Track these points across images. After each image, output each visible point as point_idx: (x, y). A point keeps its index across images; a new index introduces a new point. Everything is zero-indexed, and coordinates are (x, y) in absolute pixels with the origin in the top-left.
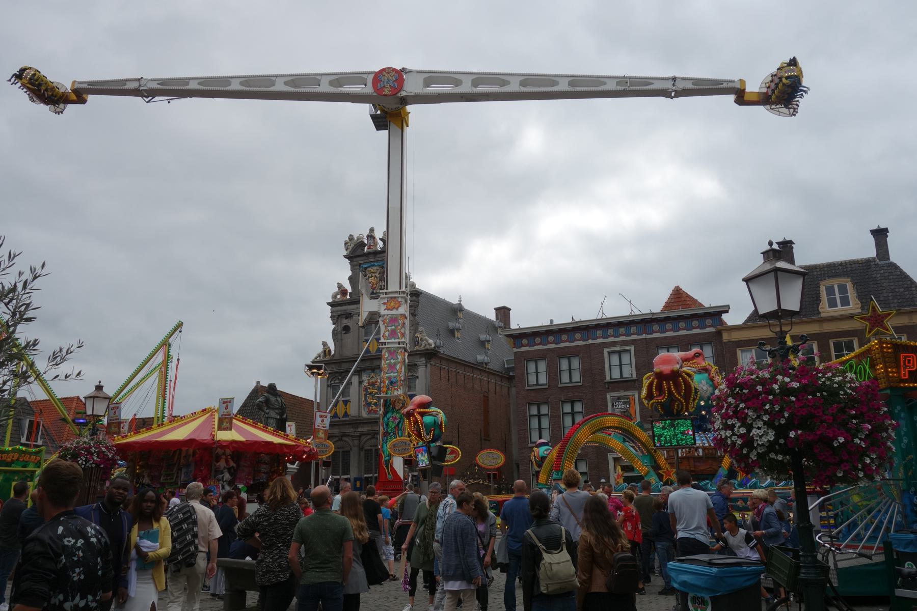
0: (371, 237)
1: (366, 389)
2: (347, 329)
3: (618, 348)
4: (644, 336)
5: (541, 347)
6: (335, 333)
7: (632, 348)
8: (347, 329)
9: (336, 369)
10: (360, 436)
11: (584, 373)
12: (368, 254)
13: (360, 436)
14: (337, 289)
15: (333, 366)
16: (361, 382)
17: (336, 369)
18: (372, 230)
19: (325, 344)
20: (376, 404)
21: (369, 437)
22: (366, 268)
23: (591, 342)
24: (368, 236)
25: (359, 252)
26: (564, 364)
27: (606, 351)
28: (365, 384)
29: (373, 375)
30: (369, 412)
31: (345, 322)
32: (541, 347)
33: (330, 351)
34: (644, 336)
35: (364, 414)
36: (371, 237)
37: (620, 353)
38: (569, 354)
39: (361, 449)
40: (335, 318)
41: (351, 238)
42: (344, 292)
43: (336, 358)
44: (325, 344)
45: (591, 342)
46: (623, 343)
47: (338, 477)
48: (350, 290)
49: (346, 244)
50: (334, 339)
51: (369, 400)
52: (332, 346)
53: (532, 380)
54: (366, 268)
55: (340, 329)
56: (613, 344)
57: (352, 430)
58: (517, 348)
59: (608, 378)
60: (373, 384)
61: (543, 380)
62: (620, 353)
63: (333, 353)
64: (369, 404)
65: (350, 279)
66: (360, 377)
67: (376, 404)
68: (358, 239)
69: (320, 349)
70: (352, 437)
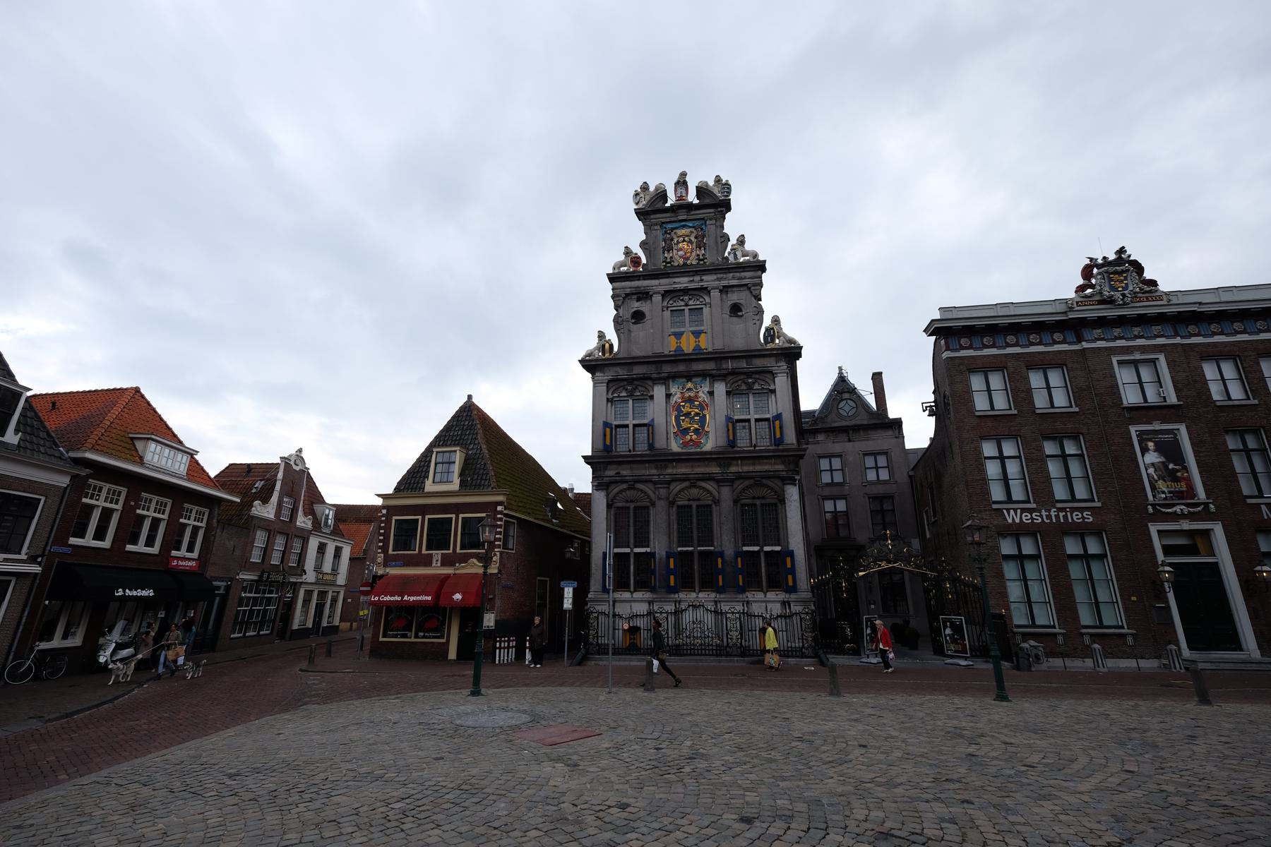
0: (682, 183)
1: (678, 408)
2: (638, 316)
3: (1138, 356)
4: (1178, 340)
5: (994, 351)
6: (618, 322)
7: (1162, 357)
8: (638, 316)
9: (622, 372)
10: (669, 483)
11: (1078, 393)
12: (674, 209)
13: (669, 483)
14: (622, 257)
15: (618, 369)
16: (668, 396)
17: (622, 372)
18: (684, 174)
19: (601, 336)
20: (696, 431)
21: (687, 484)
22: (672, 229)
23: (1085, 345)
24: (677, 184)
25: (659, 206)
26: (1036, 380)
27: (1114, 360)
28: (676, 398)
29: (689, 385)
30: (686, 444)
31: (635, 305)
32: (994, 351)
33: (611, 346)
34: (1178, 340)
35: (675, 447)
36: (682, 183)
37: (1135, 364)
38: (1043, 364)
39: (671, 503)
40: (619, 299)
41: (645, 187)
42: (636, 261)
43: (620, 356)
44: (601, 336)
45: (1085, 345)
46: (1143, 349)
47: (628, 550)
48: (644, 261)
49: (637, 194)
50: (617, 330)
51: (684, 425)
52: (612, 336)
53: (981, 404)
54: (672, 229)
55: (628, 315)
56: (1128, 350)
57: (654, 472)
58: (952, 350)
59: (1125, 402)
60: (690, 400)
61: (1001, 403)
62: (1135, 364)
63: (616, 349)
64: (685, 431)
65: (643, 245)
66: (668, 388)
67: (696, 431)
68: (657, 189)
69: (593, 343)
70: (655, 483)
